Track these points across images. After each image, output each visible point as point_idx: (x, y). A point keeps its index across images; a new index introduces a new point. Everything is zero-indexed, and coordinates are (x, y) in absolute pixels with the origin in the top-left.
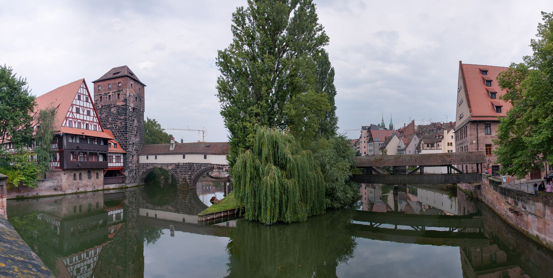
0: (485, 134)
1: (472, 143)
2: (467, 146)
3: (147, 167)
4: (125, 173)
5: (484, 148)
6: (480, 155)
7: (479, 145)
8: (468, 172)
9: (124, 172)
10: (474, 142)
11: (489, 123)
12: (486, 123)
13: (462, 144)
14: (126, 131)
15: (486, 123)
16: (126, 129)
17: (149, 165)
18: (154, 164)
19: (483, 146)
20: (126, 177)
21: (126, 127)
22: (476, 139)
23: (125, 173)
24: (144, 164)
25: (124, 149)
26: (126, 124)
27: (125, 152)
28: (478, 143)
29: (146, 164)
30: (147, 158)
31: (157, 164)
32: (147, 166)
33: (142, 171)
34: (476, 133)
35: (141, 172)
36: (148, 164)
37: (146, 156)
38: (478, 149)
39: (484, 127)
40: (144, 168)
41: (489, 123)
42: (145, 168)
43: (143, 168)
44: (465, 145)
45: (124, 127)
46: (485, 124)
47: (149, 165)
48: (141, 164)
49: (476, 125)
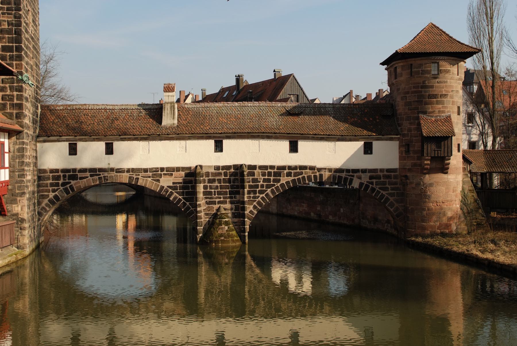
3: (73, 182)
4: (16, 209)
9: (14, 201)
14: (19, 49)
16: (18, 40)
17: (80, 175)
18: (101, 170)
20: (23, 220)
21: (18, 33)
23: (16, 209)
24: (57, 171)
25: (10, 116)
26: (19, 24)
27: (17, 127)
29: (64, 171)
30: (73, 150)
31: (112, 170)
32: (74, 177)
33: (51, 195)
35: (46, 201)
36: (74, 170)
37: (67, 144)
40: (57, 185)
42: (63, 184)
43: (52, 185)
45: (9, 32)
47: (80, 175)
48: (44, 171)
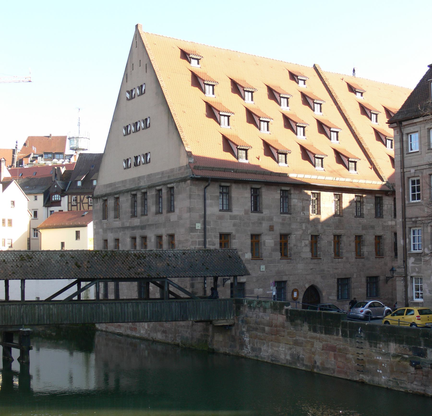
0: (220, 211)
1: (193, 229)
2: (172, 236)
5: (217, 241)
6: (230, 257)
7: (207, 234)
8: (11, 298)
10: (199, 226)
11: (228, 184)
12: (223, 184)
13: (143, 227)
15: (223, 184)
19: (215, 237)
22: (203, 219)
28: (205, 229)
34: (201, 206)
38: (205, 243)
39: (218, 194)
41: (228, 184)
44: (163, 232)
46: (220, 186)
49: (203, 187)
